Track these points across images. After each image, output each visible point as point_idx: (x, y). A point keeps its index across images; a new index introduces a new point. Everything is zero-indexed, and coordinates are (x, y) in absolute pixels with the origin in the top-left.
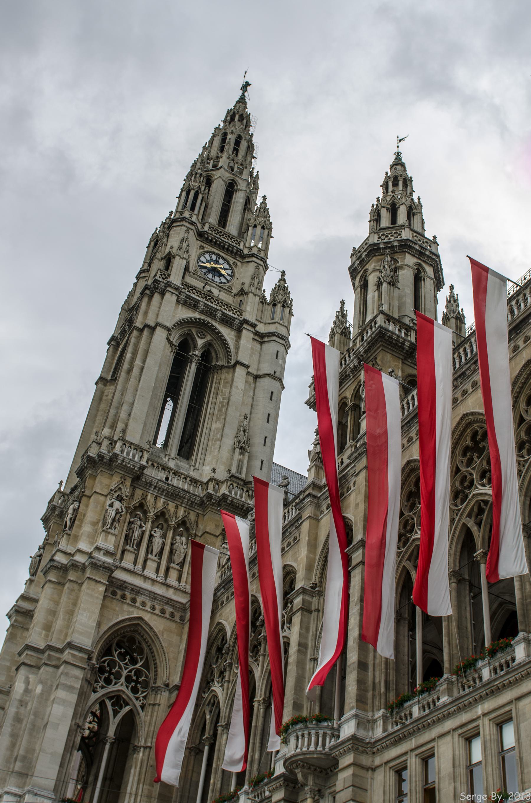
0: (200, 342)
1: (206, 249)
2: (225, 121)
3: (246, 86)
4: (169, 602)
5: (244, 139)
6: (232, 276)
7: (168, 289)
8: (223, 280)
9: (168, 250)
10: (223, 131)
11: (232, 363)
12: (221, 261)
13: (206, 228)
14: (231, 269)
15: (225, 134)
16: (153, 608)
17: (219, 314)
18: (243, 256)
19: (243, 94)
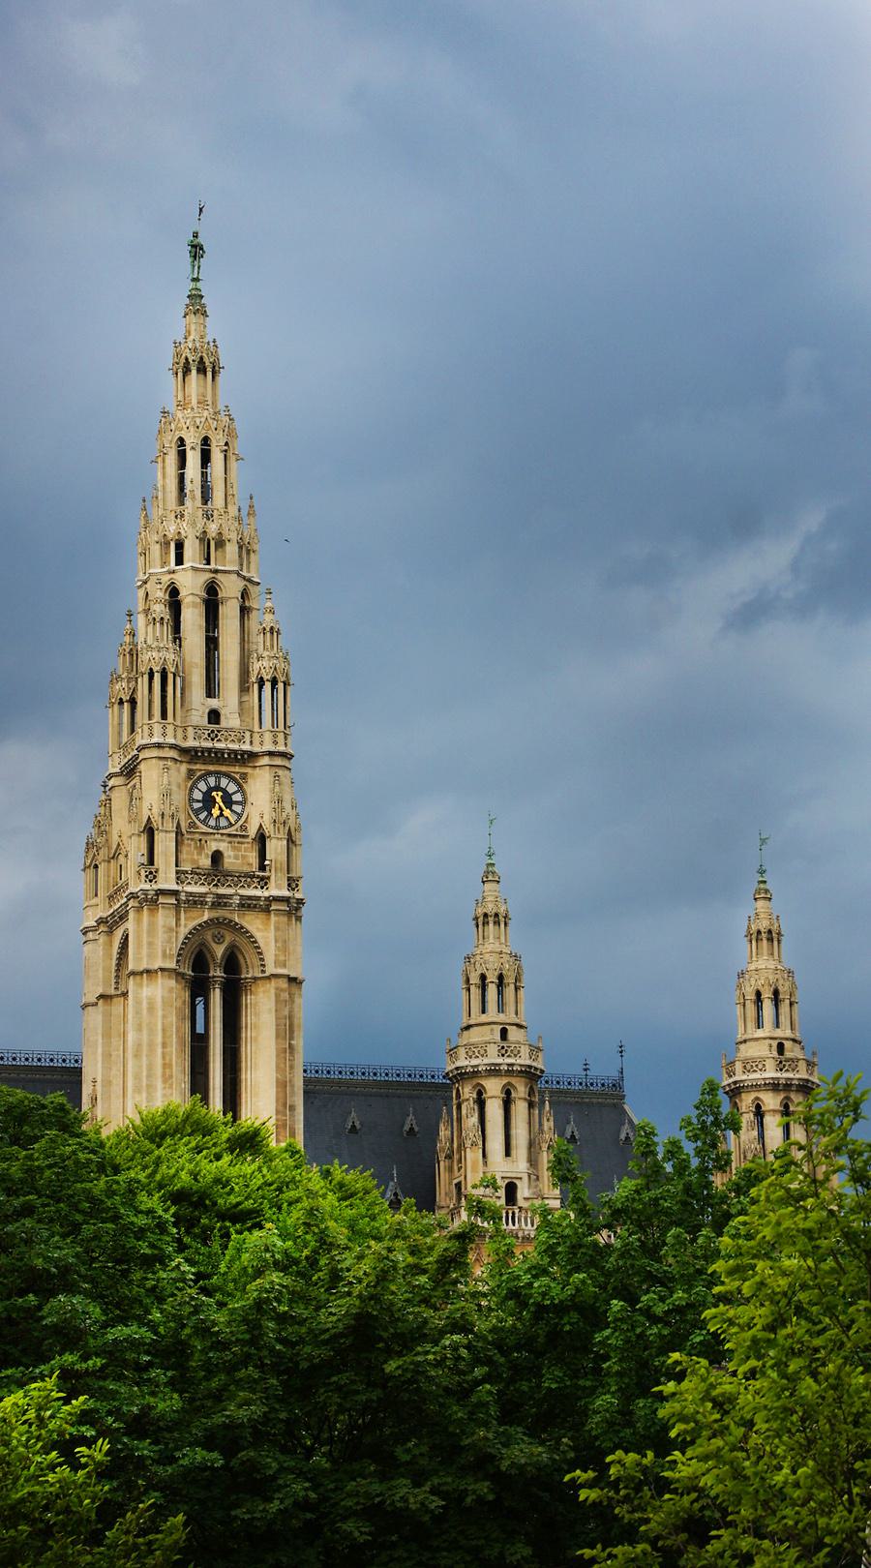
0: (219, 951)
3: (197, 250)
6: (243, 803)
12: (224, 782)
17: (236, 900)
18: (253, 756)
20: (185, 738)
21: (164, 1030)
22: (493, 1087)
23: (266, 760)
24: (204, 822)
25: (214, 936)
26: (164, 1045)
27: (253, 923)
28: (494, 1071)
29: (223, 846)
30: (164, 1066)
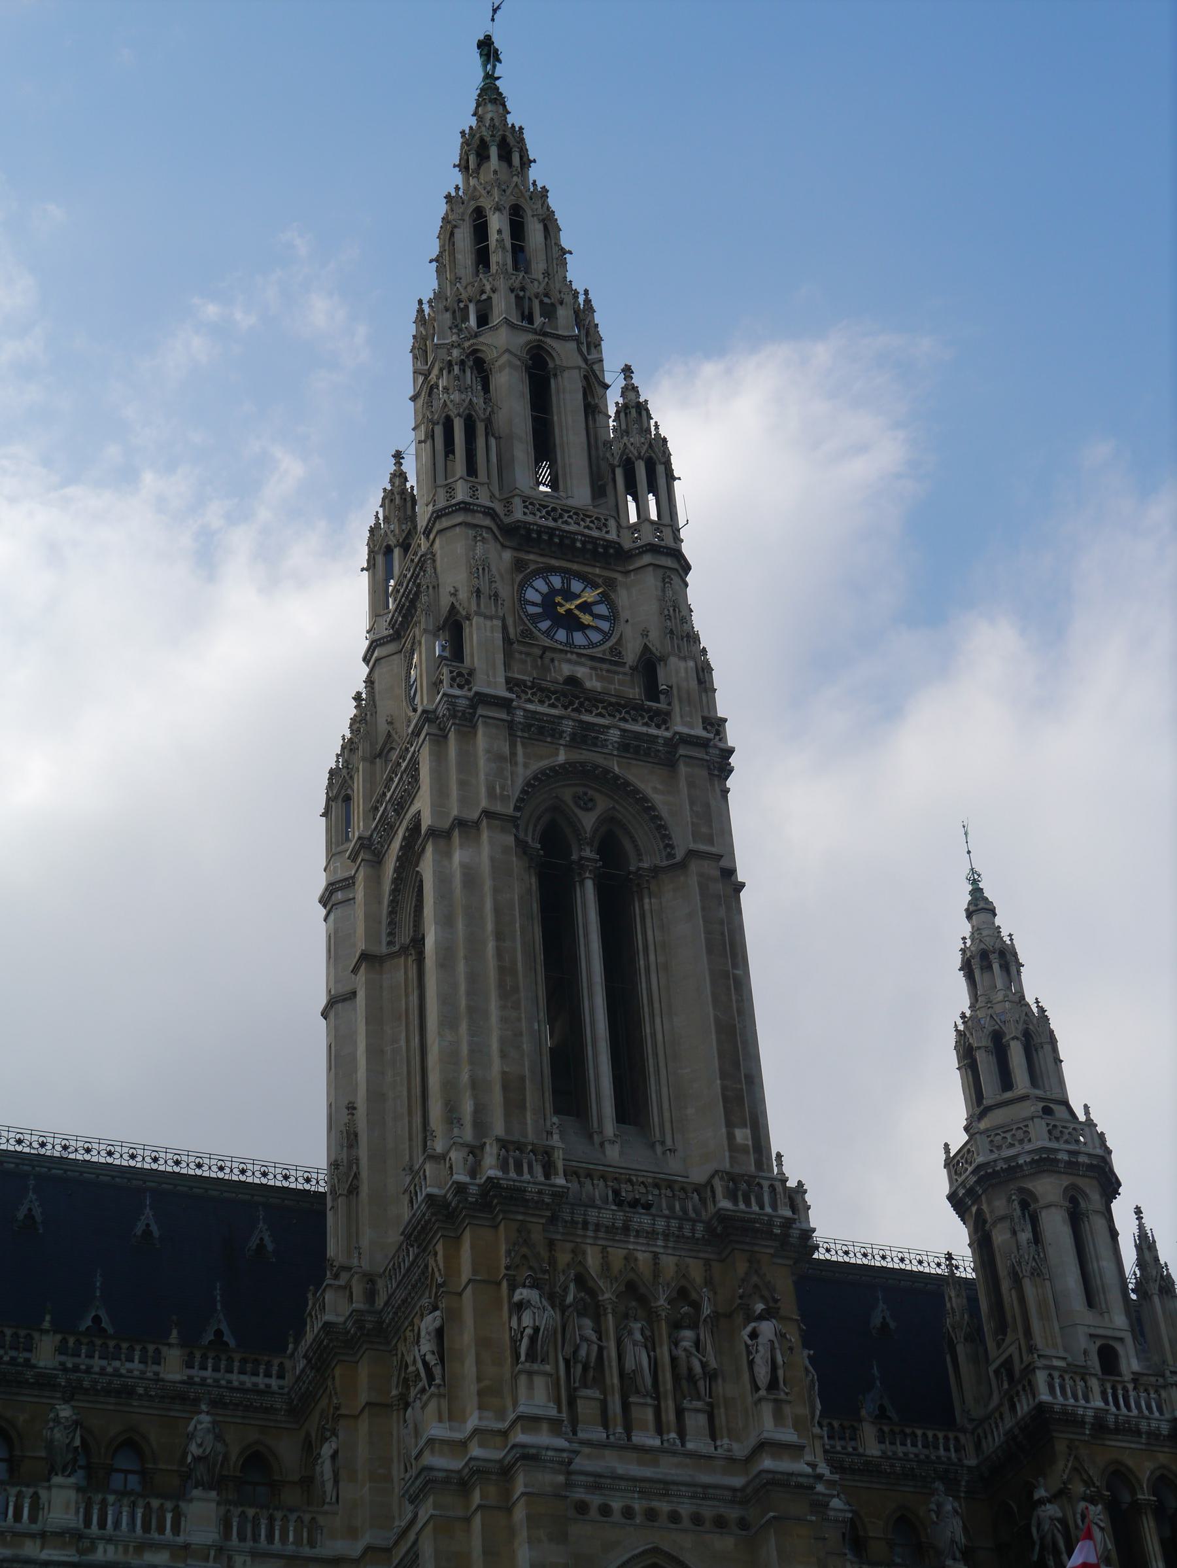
0: (588, 821)
1: (532, 567)
2: (463, 167)
3: (488, 50)
4: (704, 1492)
5: (529, 213)
6: (613, 618)
7: (481, 711)
8: (595, 637)
9: (445, 601)
10: (473, 205)
11: (680, 854)
12: (576, 586)
13: (518, 514)
14: (605, 598)
15: (479, 213)
16: (674, 1517)
17: (614, 735)
19: (490, 80)
20: (509, 513)
21: (497, 911)
22: (1048, 1188)
23: (647, 559)
24: (547, 633)
25: (576, 798)
26: (499, 936)
27: (647, 781)
28: (1045, 1163)
29: (581, 672)
30: (501, 970)
